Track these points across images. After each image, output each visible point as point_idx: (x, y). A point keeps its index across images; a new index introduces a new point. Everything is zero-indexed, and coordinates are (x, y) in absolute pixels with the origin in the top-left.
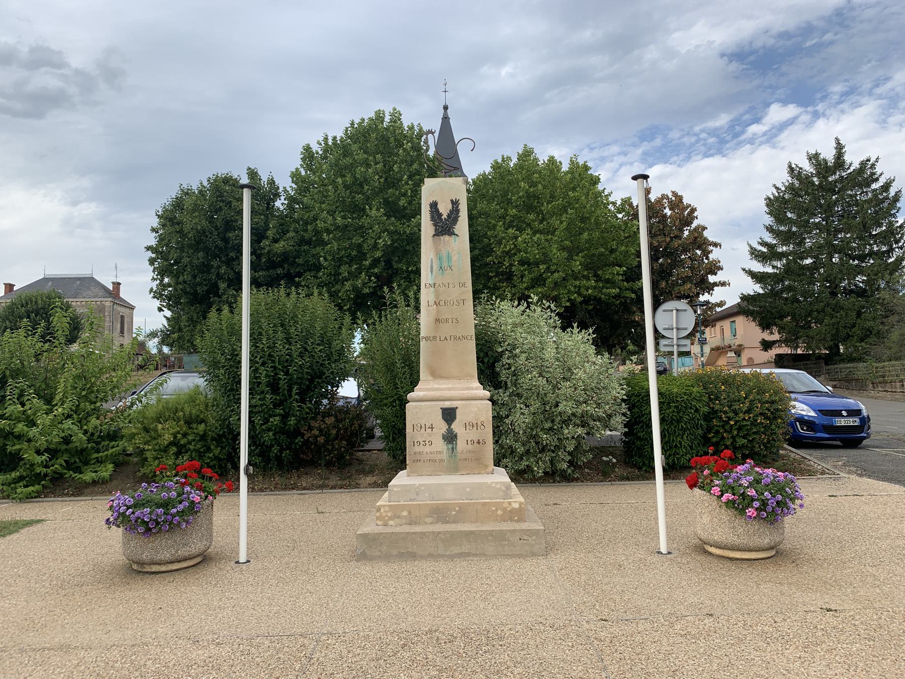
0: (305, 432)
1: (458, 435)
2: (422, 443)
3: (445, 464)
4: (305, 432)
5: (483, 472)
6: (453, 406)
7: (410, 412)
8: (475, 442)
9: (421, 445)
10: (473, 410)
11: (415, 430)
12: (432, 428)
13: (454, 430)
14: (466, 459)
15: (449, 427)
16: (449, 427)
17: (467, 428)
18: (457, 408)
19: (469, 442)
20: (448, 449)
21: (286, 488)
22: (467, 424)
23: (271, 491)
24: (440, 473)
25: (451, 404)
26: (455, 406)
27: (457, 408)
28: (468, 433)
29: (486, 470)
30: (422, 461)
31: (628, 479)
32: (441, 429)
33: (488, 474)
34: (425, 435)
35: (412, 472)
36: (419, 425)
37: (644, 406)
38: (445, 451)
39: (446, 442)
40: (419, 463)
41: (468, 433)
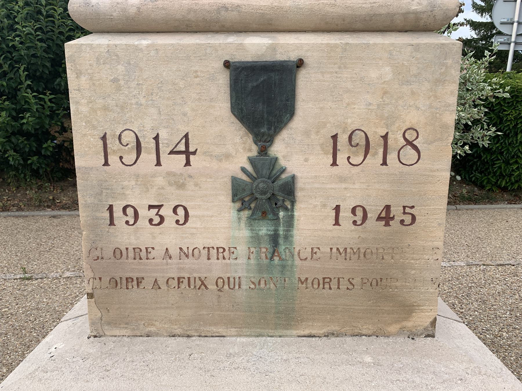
0: (57, 135)
1: (299, 184)
2: (143, 213)
3: (241, 295)
4: (57, 135)
5: (393, 328)
6: (280, 57)
7: (83, 79)
8: (372, 216)
9: (143, 222)
10: (373, 74)
11: (113, 159)
12: (187, 153)
13: (282, 162)
14: (326, 281)
15: (263, 151)
16: (263, 151)
17: (341, 158)
18: (300, 63)
19: (345, 214)
20: (256, 239)
21: (41, 205)
22: (343, 139)
23: (20, 209)
24: (222, 330)
25: (273, 48)
26: (293, 56)
27: (300, 63)
28: (342, 179)
29: (409, 324)
30: (148, 283)
31: (476, 202)
32: (228, 156)
33: (412, 336)
34: (160, 181)
35: (113, 323)
36: (129, 138)
37: (505, 111)
38: (242, 249)
39: (246, 213)
40: (134, 293)
41: (342, 179)
